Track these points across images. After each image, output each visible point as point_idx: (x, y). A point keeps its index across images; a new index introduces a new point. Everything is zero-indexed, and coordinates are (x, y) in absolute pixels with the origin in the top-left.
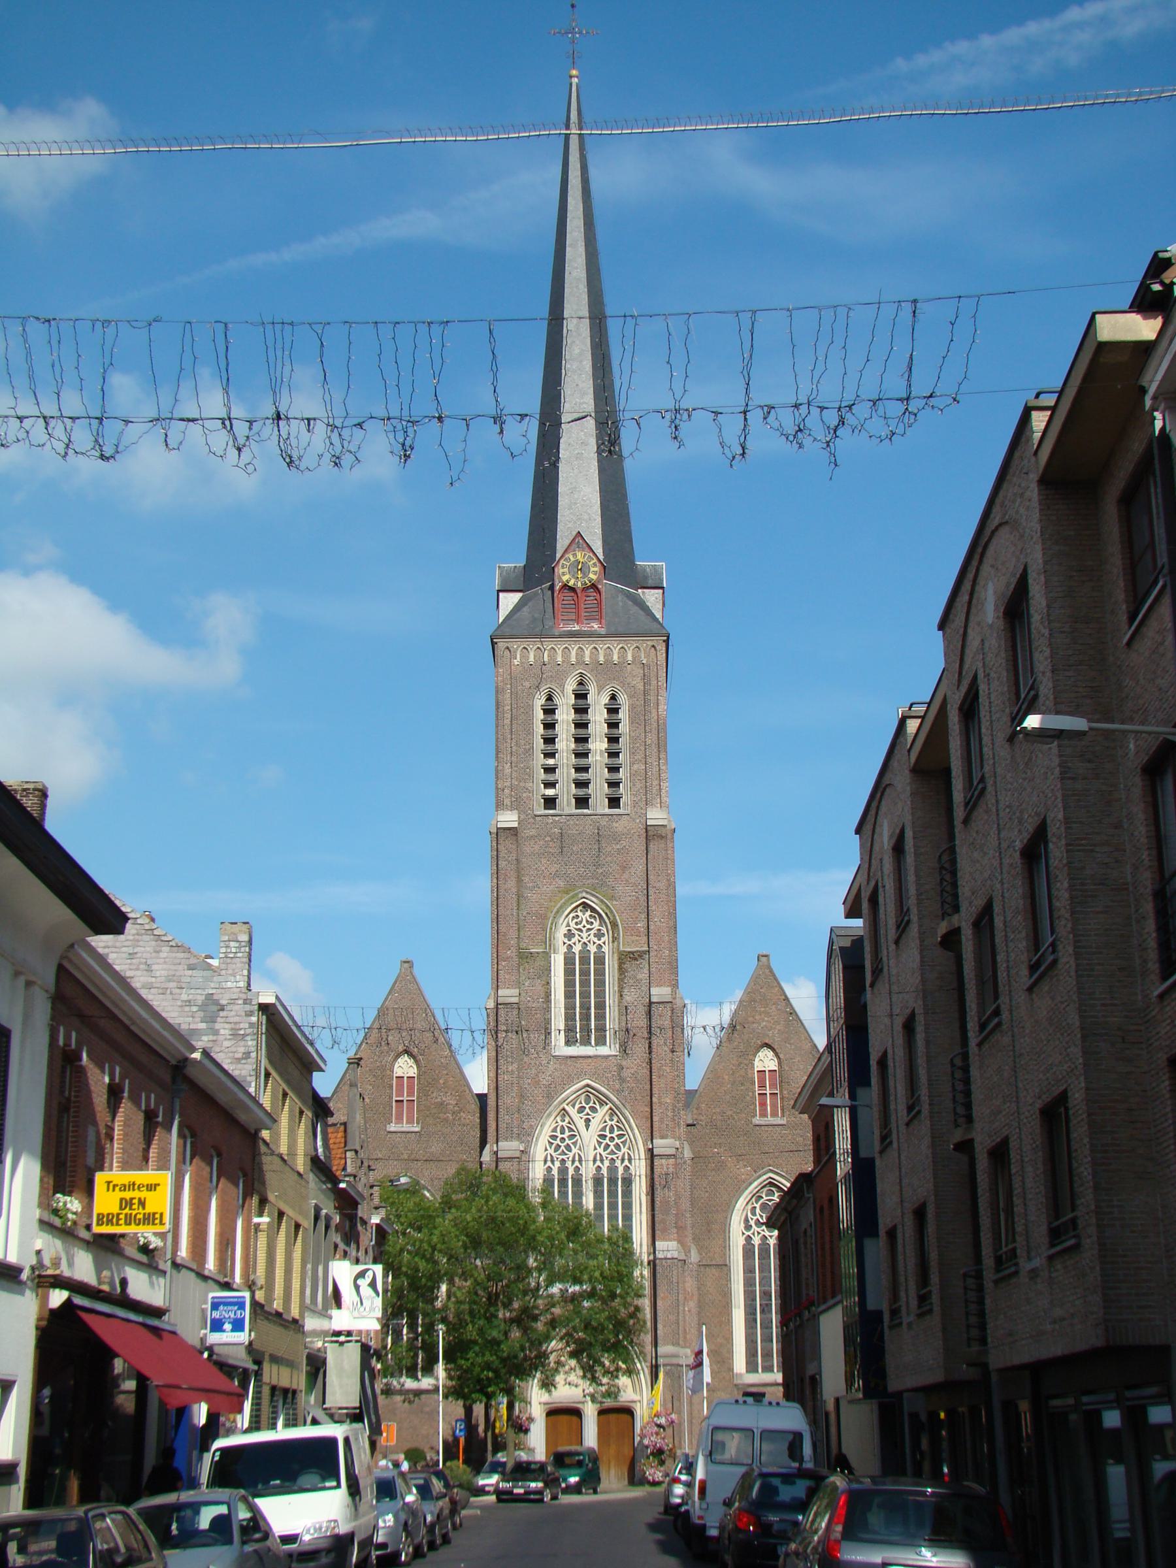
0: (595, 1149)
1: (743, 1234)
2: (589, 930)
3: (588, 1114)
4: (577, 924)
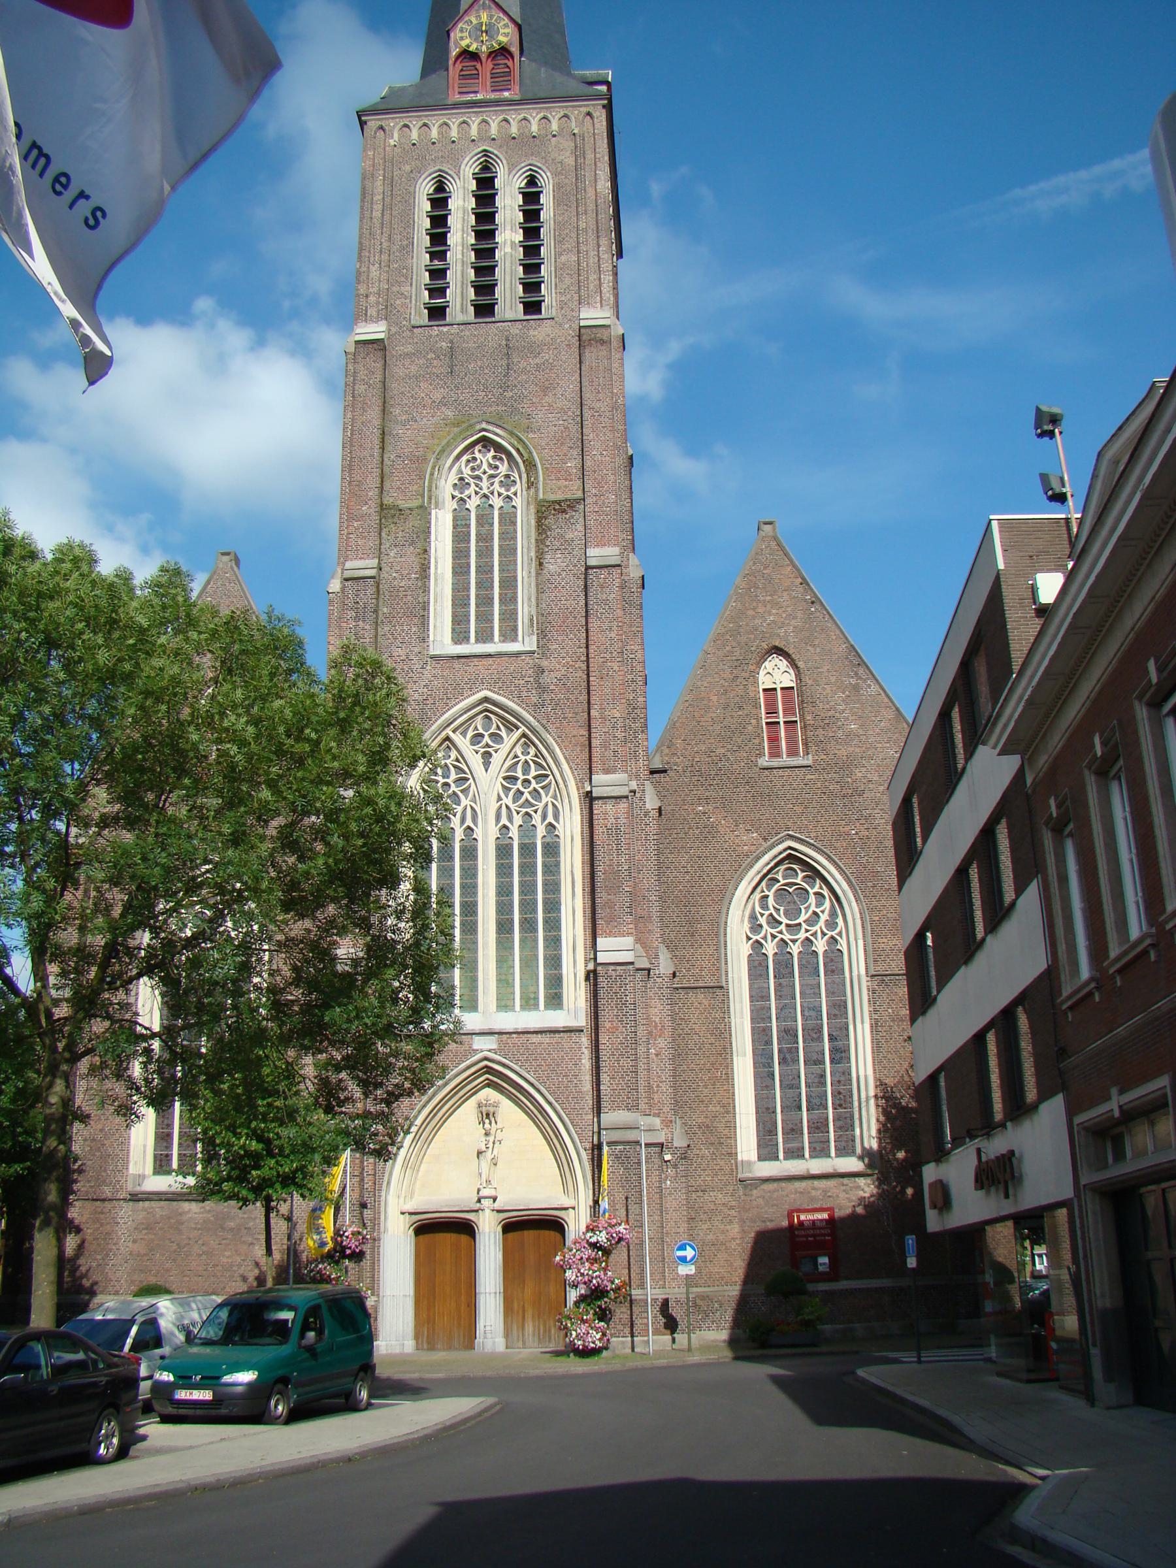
0: (499, 799)
1: (749, 938)
2: (492, 476)
3: (488, 745)
4: (473, 469)
